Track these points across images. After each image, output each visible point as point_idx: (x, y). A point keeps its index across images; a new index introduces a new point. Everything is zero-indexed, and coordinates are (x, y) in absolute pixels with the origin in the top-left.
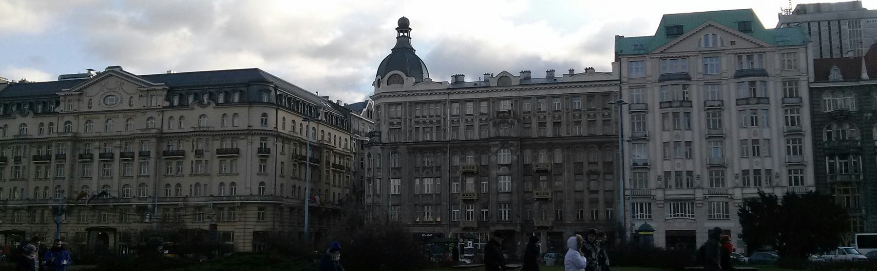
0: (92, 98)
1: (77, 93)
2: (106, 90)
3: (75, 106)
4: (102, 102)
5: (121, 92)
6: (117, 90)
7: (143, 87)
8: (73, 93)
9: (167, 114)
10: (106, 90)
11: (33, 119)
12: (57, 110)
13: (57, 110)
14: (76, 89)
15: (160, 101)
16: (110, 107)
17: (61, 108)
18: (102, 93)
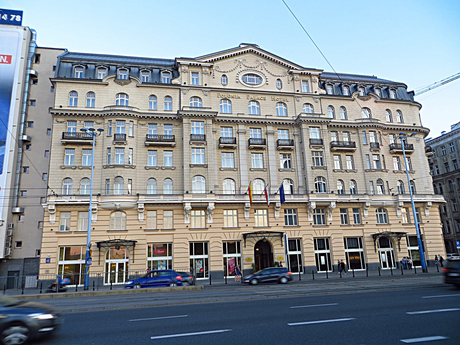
1: (209, 64)
2: (243, 68)
3: (204, 80)
4: (240, 79)
5: (264, 72)
7: (296, 69)
8: (202, 64)
9: (326, 103)
10: (243, 68)
11: (138, 89)
12: (175, 81)
13: (175, 81)
14: (208, 60)
15: (316, 87)
17: (184, 78)
18: (239, 70)
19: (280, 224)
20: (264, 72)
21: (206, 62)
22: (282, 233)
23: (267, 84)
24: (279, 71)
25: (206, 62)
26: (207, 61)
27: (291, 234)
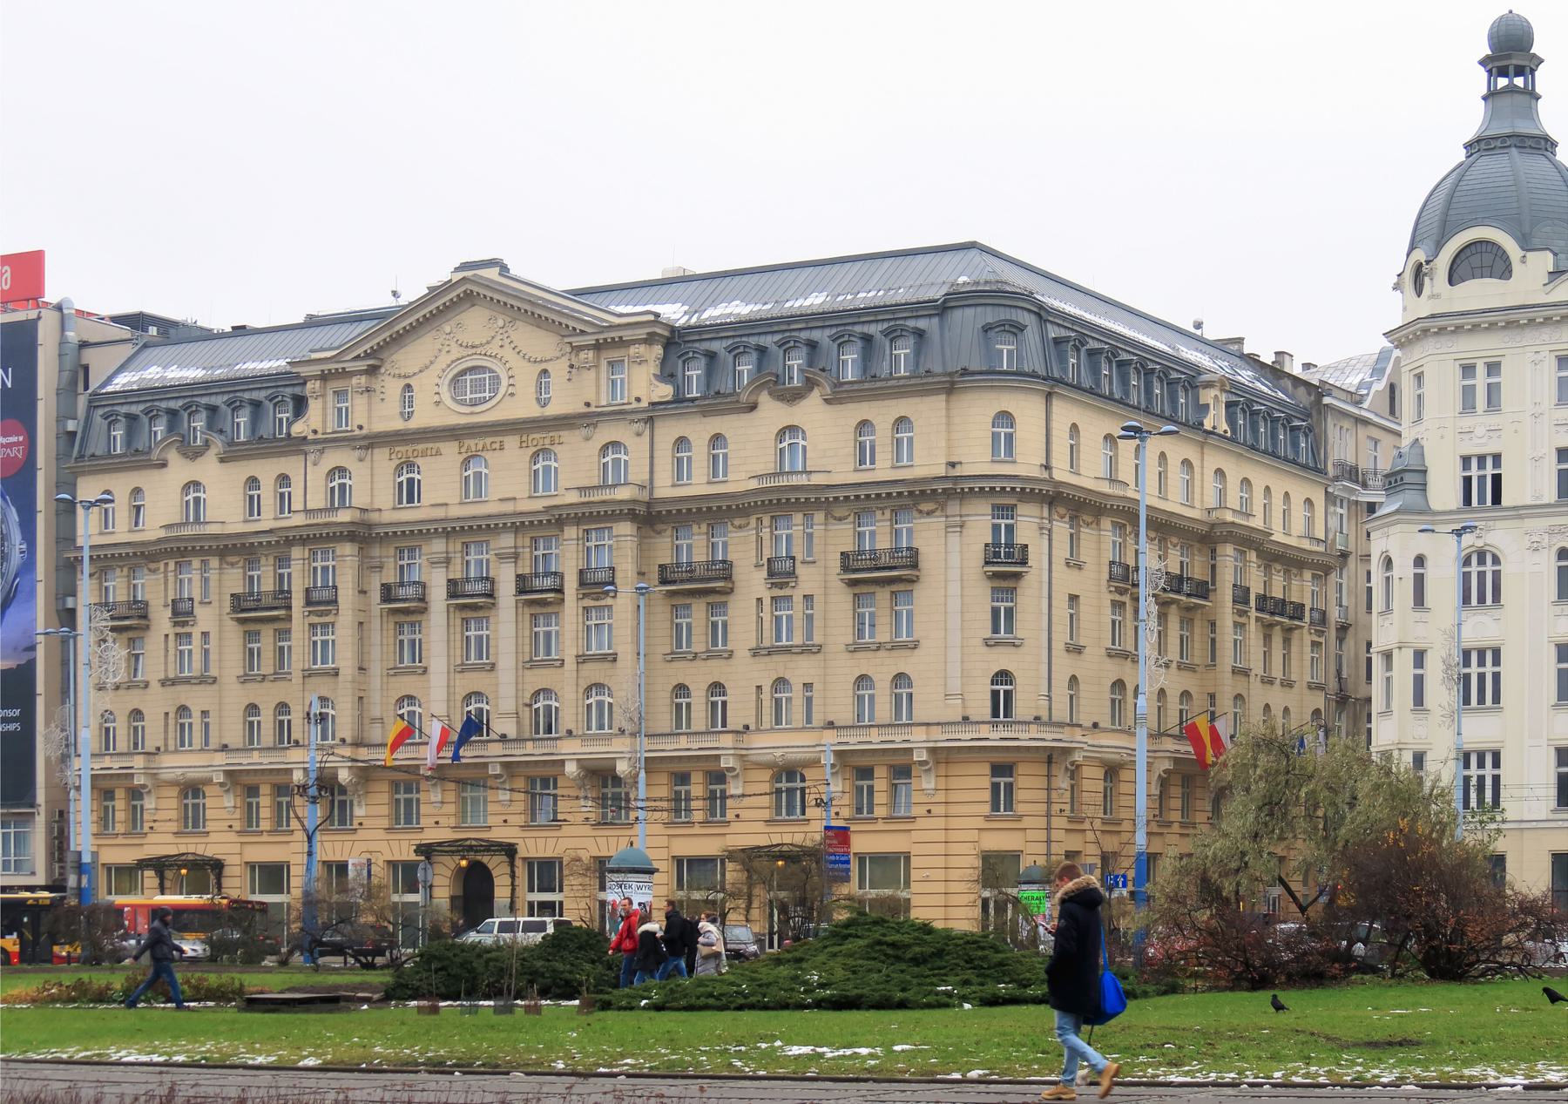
0: (411, 381)
1: (362, 365)
2: (456, 352)
5: (508, 353)
6: (493, 348)
8: (350, 367)
10: (456, 352)
12: (298, 428)
13: (298, 428)
14: (360, 351)
16: (472, 413)
19: (512, 819)
20: (508, 353)
21: (357, 358)
22: (512, 845)
23: (512, 395)
24: (541, 344)
25: (357, 358)
26: (358, 356)
27: (535, 846)
